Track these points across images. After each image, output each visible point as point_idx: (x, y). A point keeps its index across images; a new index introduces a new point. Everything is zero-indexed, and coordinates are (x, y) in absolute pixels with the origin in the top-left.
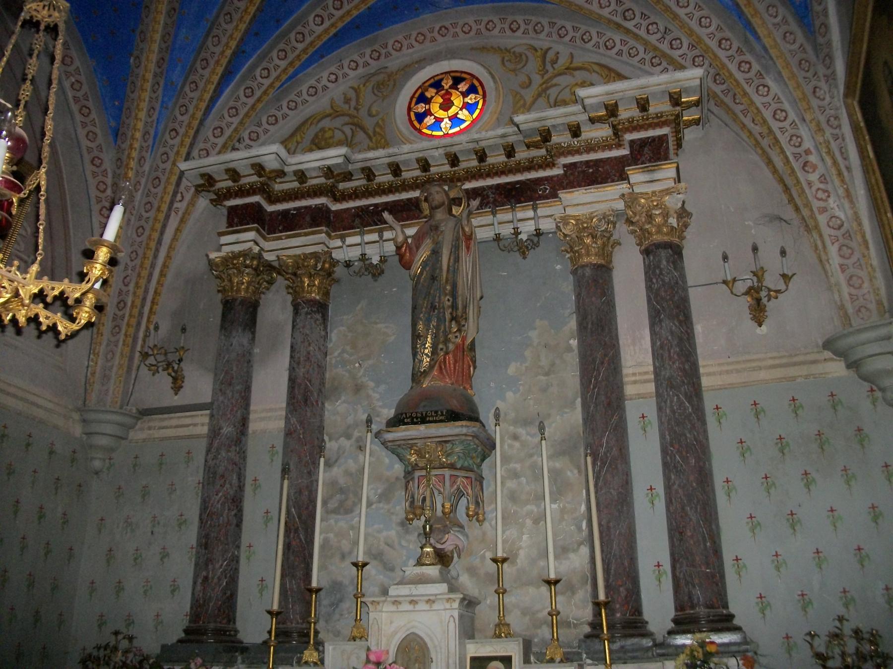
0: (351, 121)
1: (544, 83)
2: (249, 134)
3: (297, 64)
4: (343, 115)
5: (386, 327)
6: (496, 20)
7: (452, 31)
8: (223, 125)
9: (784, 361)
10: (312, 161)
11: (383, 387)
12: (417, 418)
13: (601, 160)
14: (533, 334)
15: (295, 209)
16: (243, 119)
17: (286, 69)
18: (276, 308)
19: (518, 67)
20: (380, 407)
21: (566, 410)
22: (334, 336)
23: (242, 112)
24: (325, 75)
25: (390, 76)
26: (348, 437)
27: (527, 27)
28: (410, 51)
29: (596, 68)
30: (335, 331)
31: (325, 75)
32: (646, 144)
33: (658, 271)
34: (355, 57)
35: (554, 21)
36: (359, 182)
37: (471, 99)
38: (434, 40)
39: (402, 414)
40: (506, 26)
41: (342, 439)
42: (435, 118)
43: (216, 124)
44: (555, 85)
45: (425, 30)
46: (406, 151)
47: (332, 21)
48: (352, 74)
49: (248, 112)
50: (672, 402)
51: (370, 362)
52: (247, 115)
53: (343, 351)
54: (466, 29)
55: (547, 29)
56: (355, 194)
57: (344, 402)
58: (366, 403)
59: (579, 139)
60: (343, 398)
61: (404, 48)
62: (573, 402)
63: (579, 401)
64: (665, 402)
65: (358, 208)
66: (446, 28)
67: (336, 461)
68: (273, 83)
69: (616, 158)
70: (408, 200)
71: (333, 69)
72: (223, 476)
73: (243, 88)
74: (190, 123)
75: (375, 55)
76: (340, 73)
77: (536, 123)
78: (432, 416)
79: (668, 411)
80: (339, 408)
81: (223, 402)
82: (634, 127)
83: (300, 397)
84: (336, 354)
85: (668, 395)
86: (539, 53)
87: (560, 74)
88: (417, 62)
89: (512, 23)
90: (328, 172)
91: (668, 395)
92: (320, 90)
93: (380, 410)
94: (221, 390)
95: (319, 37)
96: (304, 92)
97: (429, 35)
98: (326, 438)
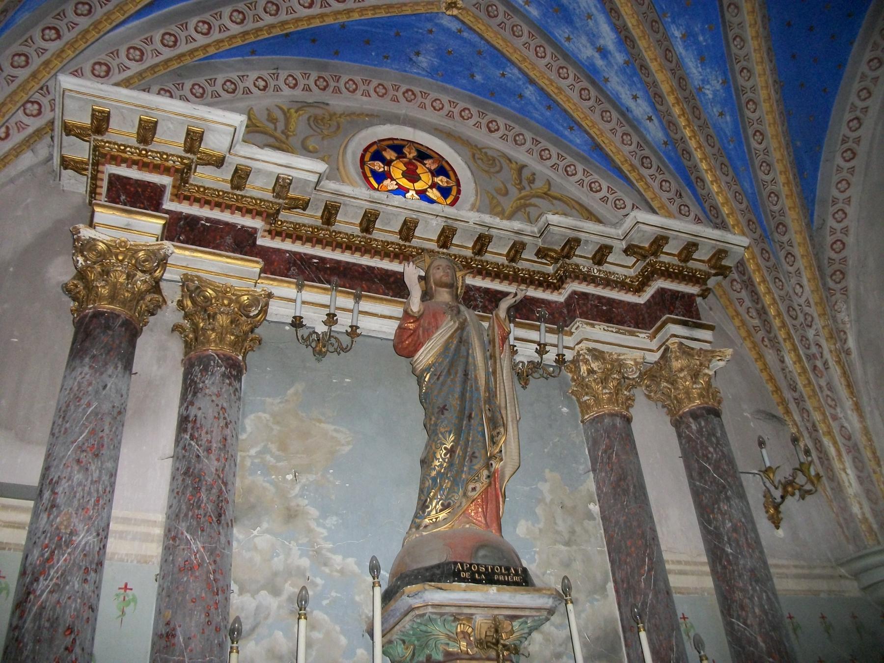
0: (277, 144)
1: (521, 198)
2: (194, 85)
3: (226, 46)
4: (262, 132)
5: (335, 430)
6: (474, 111)
7: (420, 99)
8: (114, 64)
9: (806, 571)
10: (269, 163)
11: (332, 521)
12: (480, 574)
13: (614, 300)
14: (545, 487)
15: (208, 220)
16: (145, 71)
17: (234, 37)
18: (158, 356)
19: (492, 170)
20: (330, 550)
21: (597, 597)
22: (250, 423)
23: (150, 61)
24: (253, 75)
25: (332, 115)
26: (275, 592)
27: (507, 133)
28: (364, 98)
29: (577, 207)
30: (252, 416)
31: (253, 75)
32: (677, 298)
33: (714, 440)
34: (297, 74)
35: (538, 139)
36: (311, 218)
37: (441, 181)
38: (395, 100)
39: (455, 563)
40: (484, 122)
41: (263, 593)
42: (397, 184)
43: (103, 58)
44: (535, 206)
45: (388, 84)
46: (396, 204)
47: (324, 10)
48: (287, 91)
49: (157, 65)
50: (760, 598)
51: (312, 477)
52: (153, 68)
53: (265, 450)
54: (437, 105)
55: (529, 144)
56: (295, 235)
57: (267, 531)
58: (305, 540)
59: (601, 268)
60: (265, 525)
61: (359, 92)
62: (604, 588)
63: (611, 586)
64: (751, 599)
65: (295, 254)
66: (413, 94)
67: (253, 629)
68: (209, 45)
69: (629, 303)
70: (369, 268)
71: (265, 74)
72: (70, 630)
73: (162, 31)
74: (87, 31)
75: (322, 84)
76: (272, 83)
77: (569, 231)
78: (502, 574)
79: (757, 610)
80: (257, 540)
81: (80, 484)
82: (668, 273)
83: (210, 507)
84: (253, 452)
85: (754, 589)
86: (514, 166)
87: (538, 197)
88: (367, 115)
89: (491, 122)
90: (282, 186)
91: (754, 589)
92: (240, 90)
93: (329, 555)
94: (78, 461)
95: (298, 20)
96: (220, 82)
97: (391, 92)
98: (234, 587)
